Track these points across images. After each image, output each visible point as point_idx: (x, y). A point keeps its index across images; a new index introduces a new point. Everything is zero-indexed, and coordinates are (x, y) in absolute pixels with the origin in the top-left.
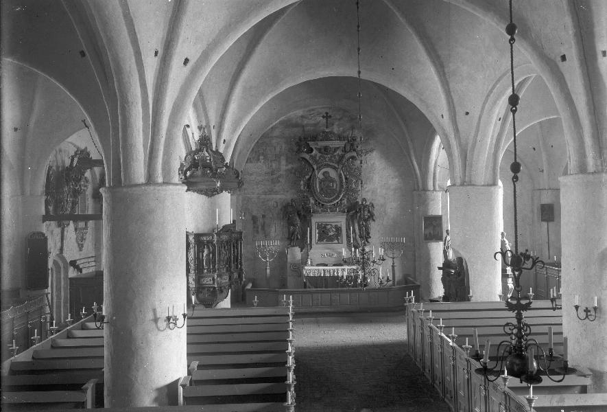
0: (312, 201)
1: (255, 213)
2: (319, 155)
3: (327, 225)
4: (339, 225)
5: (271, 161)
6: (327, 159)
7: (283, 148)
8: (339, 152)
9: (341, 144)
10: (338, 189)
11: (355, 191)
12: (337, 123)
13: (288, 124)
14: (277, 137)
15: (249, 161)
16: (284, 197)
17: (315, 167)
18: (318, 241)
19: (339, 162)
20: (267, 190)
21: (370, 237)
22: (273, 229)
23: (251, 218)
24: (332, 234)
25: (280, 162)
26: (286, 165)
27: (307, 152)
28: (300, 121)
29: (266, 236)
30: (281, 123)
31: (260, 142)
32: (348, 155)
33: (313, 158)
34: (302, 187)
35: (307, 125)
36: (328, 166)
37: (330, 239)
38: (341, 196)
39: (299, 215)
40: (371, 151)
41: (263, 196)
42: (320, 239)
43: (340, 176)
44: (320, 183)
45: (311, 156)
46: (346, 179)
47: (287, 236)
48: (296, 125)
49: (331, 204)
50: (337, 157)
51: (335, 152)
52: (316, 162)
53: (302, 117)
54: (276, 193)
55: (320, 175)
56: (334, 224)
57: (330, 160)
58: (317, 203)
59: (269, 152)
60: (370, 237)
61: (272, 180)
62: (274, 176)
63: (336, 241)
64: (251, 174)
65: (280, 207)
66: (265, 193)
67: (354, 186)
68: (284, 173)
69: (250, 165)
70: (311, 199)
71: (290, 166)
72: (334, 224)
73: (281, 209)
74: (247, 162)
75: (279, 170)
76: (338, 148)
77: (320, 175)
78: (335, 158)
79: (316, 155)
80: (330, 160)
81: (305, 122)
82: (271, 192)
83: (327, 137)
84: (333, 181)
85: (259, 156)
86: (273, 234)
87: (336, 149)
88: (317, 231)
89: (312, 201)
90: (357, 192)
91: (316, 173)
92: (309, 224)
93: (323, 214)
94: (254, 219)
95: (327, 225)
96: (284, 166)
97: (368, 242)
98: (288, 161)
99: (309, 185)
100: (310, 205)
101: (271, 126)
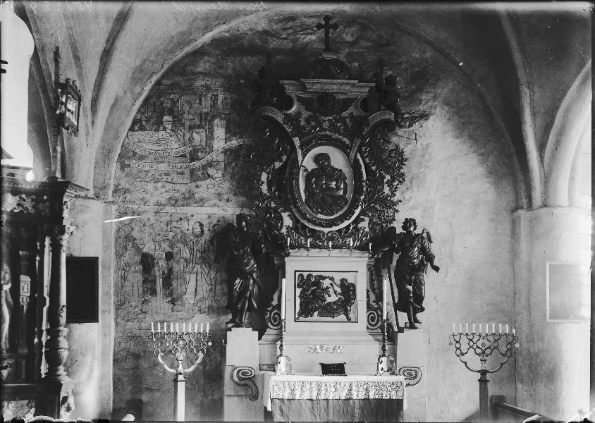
0: (288, 222)
1: (148, 248)
2: (305, 114)
3: (324, 278)
4: (350, 278)
5: (191, 128)
6: (326, 125)
7: (221, 97)
9: (361, 90)
10: (349, 196)
11: (389, 204)
12: (346, 50)
13: (229, 46)
14: (205, 74)
15: (137, 125)
16: (223, 212)
17: (297, 141)
18: (300, 315)
19: (354, 133)
20: (177, 195)
21: (422, 309)
22: (191, 287)
23: (138, 258)
24: (332, 298)
25: (210, 137)
26: (227, 140)
27: (280, 109)
28: (258, 42)
29: (173, 302)
30: (217, 42)
31: (166, 82)
32: (376, 117)
34: (264, 188)
35: (277, 51)
37: (329, 311)
38: (357, 212)
39: (256, 253)
40: (424, 116)
41: (169, 209)
43: (355, 166)
44: (308, 179)
45: (288, 118)
47: (224, 302)
48: (251, 50)
49: (334, 228)
52: (299, 131)
53: (265, 32)
54: (202, 202)
55: (308, 163)
56: (338, 277)
57: (333, 128)
58: (298, 227)
59: (186, 108)
60: (422, 309)
61: (192, 172)
62: (197, 164)
63: (343, 317)
64: (142, 158)
65: (207, 236)
66: (174, 202)
67: (387, 190)
68: (221, 158)
69: (138, 135)
70: (285, 215)
71: (234, 143)
73: (211, 241)
74: (132, 129)
75: (209, 148)
77: (308, 163)
78: (345, 123)
79: (299, 114)
81: (274, 43)
82: (189, 199)
83: (328, 70)
84: (338, 175)
85: (162, 116)
86: (189, 299)
87: (346, 103)
88: (299, 291)
89: (288, 222)
90: (395, 204)
91: (300, 158)
92: (281, 271)
93: (314, 252)
94: (147, 262)
95: (324, 278)
96: (221, 140)
97: (416, 321)
98: (230, 132)
99: (284, 181)
100: (284, 230)
101: (189, 49)
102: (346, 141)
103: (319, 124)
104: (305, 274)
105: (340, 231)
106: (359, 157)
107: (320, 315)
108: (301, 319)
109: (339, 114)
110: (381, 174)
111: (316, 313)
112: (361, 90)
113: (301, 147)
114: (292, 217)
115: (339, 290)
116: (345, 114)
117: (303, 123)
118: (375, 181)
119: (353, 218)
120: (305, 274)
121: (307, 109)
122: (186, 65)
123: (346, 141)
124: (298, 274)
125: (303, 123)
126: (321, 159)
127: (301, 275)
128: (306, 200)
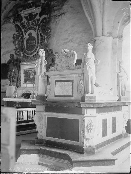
2: (26, 21)
3: (30, 71)
6: (31, 23)
8: (38, 17)
9: (38, 10)
10: (36, 44)
17: (23, 30)
24: (32, 77)
33: (22, 24)
36: (31, 28)
42: (25, 81)
43: (38, 35)
44: (27, 41)
46: (41, 36)
50: (36, 21)
51: (35, 17)
55: (26, 36)
56: (33, 70)
57: (33, 24)
58: (25, 56)
67: (46, 41)
72: (33, 70)
76: (37, 14)
77: (26, 36)
80: (33, 24)
84: (34, 39)
87: (36, 15)
88: (24, 75)
89: (22, 55)
95: (30, 71)
102: (35, 27)
103: (29, 23)
104: (25, 70)
105: (33, 56)
106: (38, 31)
107: (29, 82)
108: (25, 83)
109: (34, 19)
110: (44, 36)
111: (28, 81)
112: (38, 10)
113: (25, 31)
114: (23, 53)
115: (33, 74)
116: (35, 19)
117: (25, 24)
118: (43, 39)
119: (37, 51)
120: (25, 70)
121: (27, 20)
122: (8, 15)
123: (35, 27)
124: (24, 70)
125: (25, 24)
126: (30, 34)
127: (24, 70)
128: (26, 47)
